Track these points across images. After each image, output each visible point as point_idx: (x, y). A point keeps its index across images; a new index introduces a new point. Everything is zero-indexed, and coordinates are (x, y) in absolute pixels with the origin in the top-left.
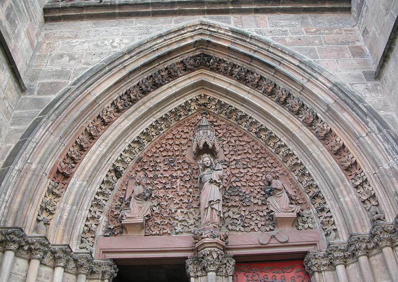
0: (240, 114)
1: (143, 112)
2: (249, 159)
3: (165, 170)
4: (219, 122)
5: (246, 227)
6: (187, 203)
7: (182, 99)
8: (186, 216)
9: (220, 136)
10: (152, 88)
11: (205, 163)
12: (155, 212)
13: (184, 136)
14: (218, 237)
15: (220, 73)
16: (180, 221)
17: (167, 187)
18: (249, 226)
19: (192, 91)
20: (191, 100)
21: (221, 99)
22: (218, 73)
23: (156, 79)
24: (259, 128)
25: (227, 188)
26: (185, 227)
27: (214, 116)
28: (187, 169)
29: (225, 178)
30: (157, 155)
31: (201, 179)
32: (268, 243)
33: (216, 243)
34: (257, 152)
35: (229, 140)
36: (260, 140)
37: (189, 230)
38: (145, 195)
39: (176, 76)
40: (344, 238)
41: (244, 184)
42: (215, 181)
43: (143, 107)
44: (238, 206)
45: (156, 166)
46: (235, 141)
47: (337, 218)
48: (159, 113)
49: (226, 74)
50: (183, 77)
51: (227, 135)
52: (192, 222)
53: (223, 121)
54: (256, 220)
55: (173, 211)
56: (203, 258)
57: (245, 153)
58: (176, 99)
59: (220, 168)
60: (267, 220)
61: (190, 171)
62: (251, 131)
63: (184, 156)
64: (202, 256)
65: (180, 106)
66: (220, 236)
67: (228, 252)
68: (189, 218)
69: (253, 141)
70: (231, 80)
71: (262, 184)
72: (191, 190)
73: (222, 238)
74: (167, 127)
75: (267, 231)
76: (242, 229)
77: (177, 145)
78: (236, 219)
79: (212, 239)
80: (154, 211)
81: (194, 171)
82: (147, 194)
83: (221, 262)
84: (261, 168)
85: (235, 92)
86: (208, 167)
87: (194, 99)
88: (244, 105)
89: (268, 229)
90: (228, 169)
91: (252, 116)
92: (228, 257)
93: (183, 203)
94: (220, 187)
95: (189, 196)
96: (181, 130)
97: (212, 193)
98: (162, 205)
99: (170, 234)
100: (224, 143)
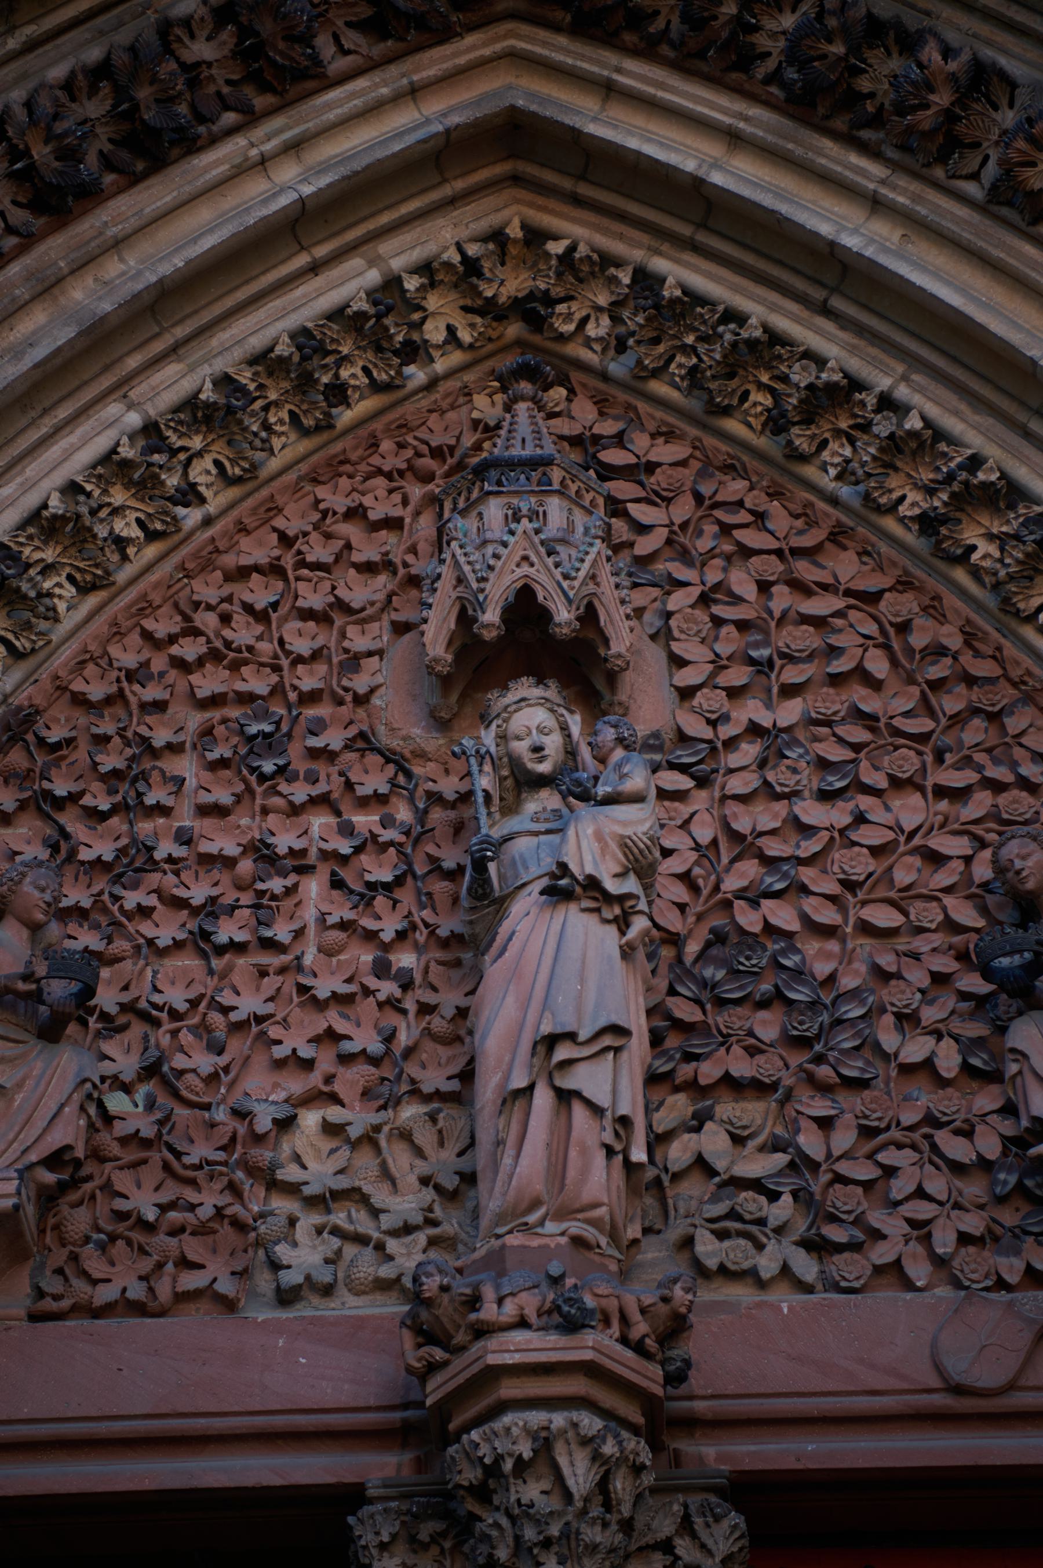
0: (801, 375)
1: (40, 353)
2: (868, 720)
3: (205, 811)
4: (640, 442)
5: (839, 1248)
6: (375, 1061)
7: (356, 262)
8: (365, 1161)
9: (645, 545)
10: (107, 163)
11: (521, 748)
12: (121, 1129)
13: (367, 551)
14: (607, 1322)
15: (647, 51)
16: (317, 1202)
17: (222, 938)
18: (854, 1247)
19: (434, 196)
20: (426, 269)
21: (660, 265)
22: (635, 53)
23: (144, 93)
24: (950, 477)
25: (692, 948)
26: (350, 1250)
27: (602, 405)
28: (380, 799)
29: (675, 865)
30: (151, 693)
31: (480, 866)
32: (1011, 1387)
33: (591, 1370)
34: (936, 671)
35: (713, 577)
36: (960, 575)
37: (386, 1271)
38: (37, 997)
39: (301, 75)
41: (828, 915)
42: (593, 884)
43: (37, 318)
44: (774, 1087)
45: (144, 776)
46: (764, 587)
48: (172, 369)
49: (701, 55)
50: (361, 83)
51: (704, 544)
53: (669, 435)
54: (920, 1193)
55: (264, 1124)
56: (482, 1493)
57: (836, 680)
58: (302, 260)
59: (637, 780)
60: (1001, 1200)
61: (404, 814)
62: (892, 509)
63: (361, 700)
64: (470, 1475)
65: (337, 314)
66: (624, 1320)
67: (686, 1446)
68: (386, 1174)
69: (904, 584)
70: (739, 106)
71: (966, 915)
72: (405, 959)
73: (640, 1328)
74: (237, 481)
75: (1001, 1284)
76: (806, 1267)
77: (307, 615)
78: (756, 1185)
79: (553, 1339)
80: (108, 1119)
81: (437, 815)
82: (59, 989)
83: (627, 1526)
84: (960, 795)
85: (767, 200)
86: (541, 782)
87: (448, 265)
88: (837, 303)
89: (1012, 1269)
90: (701, 799)
91: (902, 392)
92: (686, 1490)
93: (346, 1059)
94: (632, 933)
95: (392, 1004)
96: (340, 503)
98: (181, 1073)
99: (229, 1305)
100: (678, 600)
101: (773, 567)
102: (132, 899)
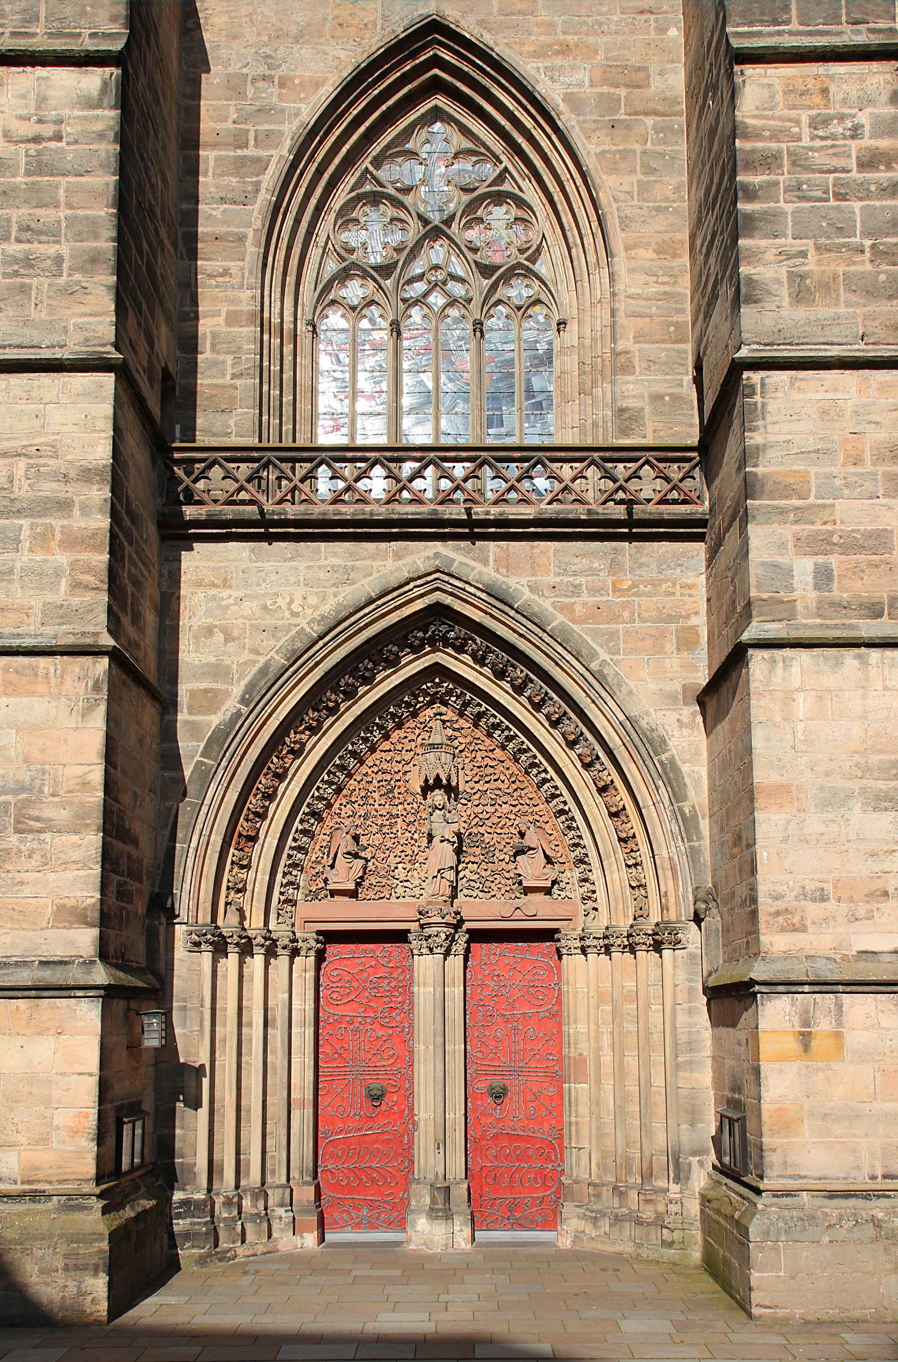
40: (603, 920)
47: (601, 895)
51: (471, 748)
52: (417, 882)
76: (481, 895)
84: (515, 806)
90: (470, 804)
97: (444, 854)
101: (484, 754)
102: (368, 823)
